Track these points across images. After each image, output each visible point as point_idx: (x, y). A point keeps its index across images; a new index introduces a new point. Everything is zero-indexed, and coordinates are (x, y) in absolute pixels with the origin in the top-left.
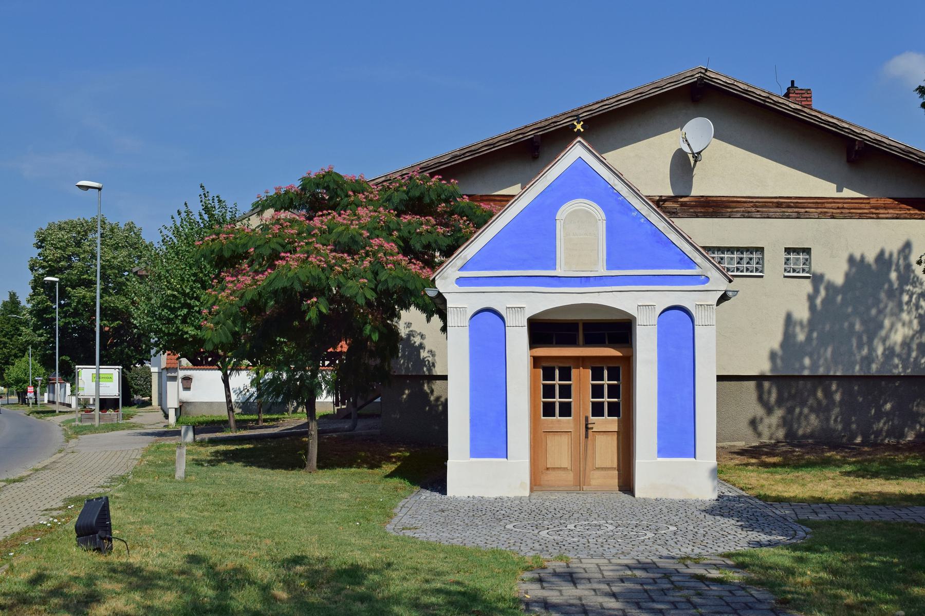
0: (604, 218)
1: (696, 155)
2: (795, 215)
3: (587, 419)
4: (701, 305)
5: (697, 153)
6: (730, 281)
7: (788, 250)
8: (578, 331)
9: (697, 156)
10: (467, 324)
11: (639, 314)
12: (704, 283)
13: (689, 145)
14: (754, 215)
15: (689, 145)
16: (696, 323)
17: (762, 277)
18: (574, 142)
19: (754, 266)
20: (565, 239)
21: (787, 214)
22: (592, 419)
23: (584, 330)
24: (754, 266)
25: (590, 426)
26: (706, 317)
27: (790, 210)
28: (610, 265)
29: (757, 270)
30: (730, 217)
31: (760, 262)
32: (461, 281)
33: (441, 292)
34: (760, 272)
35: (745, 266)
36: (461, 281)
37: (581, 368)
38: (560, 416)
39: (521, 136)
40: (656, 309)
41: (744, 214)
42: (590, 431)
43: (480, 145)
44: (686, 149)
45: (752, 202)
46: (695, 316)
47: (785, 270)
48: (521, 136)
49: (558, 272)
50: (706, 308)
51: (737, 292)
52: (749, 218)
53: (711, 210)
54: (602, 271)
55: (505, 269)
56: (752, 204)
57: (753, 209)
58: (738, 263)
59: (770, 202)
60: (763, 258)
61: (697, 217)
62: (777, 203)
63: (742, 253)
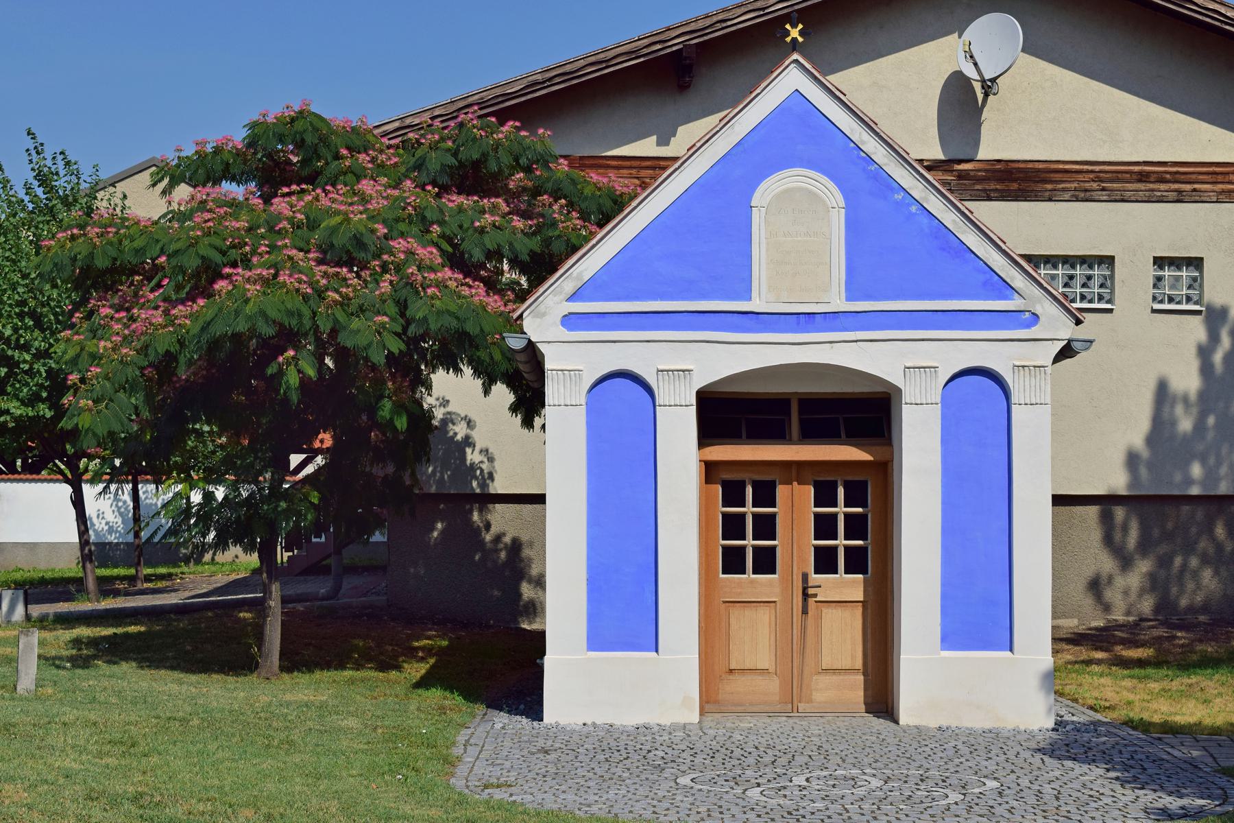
0: (842, 204)
1: (989, 83)
2: (1172, 195)
3: (805, 577)
4: (1023, 367)
5: (990, 80)
6: (1078, 322)
7: (1159, 262)
8: (789, 414)
9: (989, 87)
10: (583, 401)
11: (908, 383)
12: (1029, 325)
13: (976, 64)
14: (1096, 195)
15: (976, 64)
16: (1014, 399)
17: (1110, 311)
18: (787, 63)
19: (1096, 291)
20: (768, 244)
21: (1159, 194)
22: (815, 578)
23: (800, 413)
24: (1096, 291)
25: (811, 591)
26: (1033, 388)
27: (1163, 187)
28: (853, 290)
29: (1101, 298)
30: (1050, 200)
31: (1108, 282)
32: (570, 320)
33: (533, 339)
34: (1108, 302)
35: (1078, 291)
36: (570, 320)
37: (795, 483)
38: (754, 573)
39: (658, 47)
40: (940, 374)
41: (1077, 193)
42: (811, 601)
43: (582, 63)
44: (970, 72)
45: (1092, 172)
46: (1012, 388)
47: (1154, 298)
48: (658, 47)
49: (755, 305)
50: (1033, 373)
51: (1091, 342)
52: (1087, 200)
53: (1015, 186)
54: (838, 302)
56: (1092, 176)
57: (1095, 185)
58: (1066, 285)
59: (1126, 172)
60: (1112, 277)
61: (989, 199)
62: (1140, 173)
63: (1073, 267)
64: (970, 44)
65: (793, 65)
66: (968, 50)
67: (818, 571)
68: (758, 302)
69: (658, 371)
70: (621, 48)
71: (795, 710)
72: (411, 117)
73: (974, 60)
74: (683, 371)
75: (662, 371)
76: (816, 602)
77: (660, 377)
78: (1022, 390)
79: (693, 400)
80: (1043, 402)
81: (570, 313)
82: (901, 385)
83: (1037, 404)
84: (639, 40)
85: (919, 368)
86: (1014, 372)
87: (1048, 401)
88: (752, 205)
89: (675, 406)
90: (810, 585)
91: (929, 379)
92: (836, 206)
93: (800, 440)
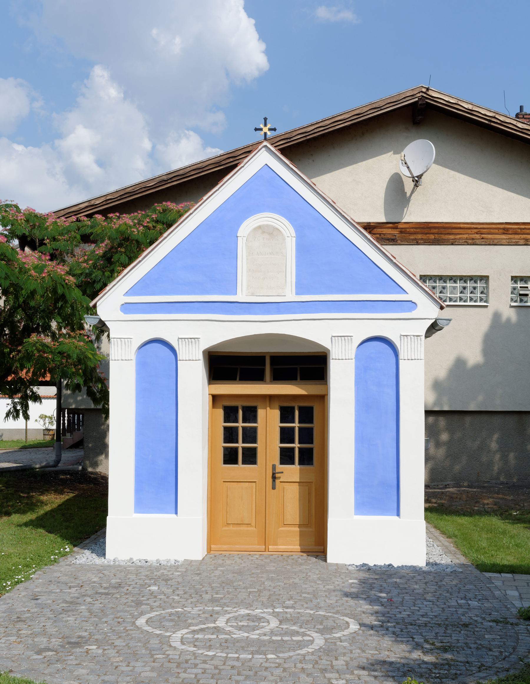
0: (294, 234)
1: (416, 179)
2: (522, 242)
3: (274, 467)
4: (407, 336)
5: (417, 177)
6: (442, 308)
7: (514, 279)
8: (264, 365)
9: (417, 181)
10: (133, 356)
11: (334, 346)
12: (410, 310)
13: (408, 168)
14: (478, 242)
15: (408, 168)
16: (401, 356)
17: (486, 306)
18: (260, 147)
19: (479, 295)
20: (247, 259)
21: (514, 241)
22: (280, 468)
23: (272, 364)
24: (479, 295)
25: (277, 475)
26: (413, 349)
27: (517, 236)
28: (300, 289)
29: (481, 300)
30: (452, 244)
31: (485, 292)
32: (127, 308)
33: (103, 319)
34: (485, 302)
35: (468, 295)
36: (127, 308)
37: (268, 408)
38: (243, 464)
39: (231, 160)
40: (353, 340)
41: (467, 240)
42: (277, 481)
43: (189, 169)
44: (404, 171)
45: (476, 228)
46: (399, 349)
47: (512, 300)
48: (231, 160)
49: (240, 297)
50: (413, 340)
51: (450, 320)
52: (473, 245)
53: (432, 237)
54: (290, 295)
55: (178, 294)
56: (476, 231)
57: (478, 236)
58: (461, 293)
59: (496, 229)
60: (487, 287)
61: (418, 244)
62: (504, 229)
63: (465, 282)
64: (404, 156)
65: (264, 149)
66: (403, 159)
67: (282, 463)
68: (241, 296)
69: (179, 338)
70: (211, 161)
71: (267, 550)
72: (94, 200)
73: (407, 165)
74: (194, 339)
75: (181, 339)
76: (281, 482)
77: (180, 343)
78: (406, 351)
79: (201, 357)
80: (419, 358)
81: (126, 303)
82: (329, 347)
83: (415, 359)
84: (220, 156)
85: (341, 337)
86: (401, 340)
87: (423, 357)
88: (238, 235)
89: (190, 360)
90: (277, 471)
91: (347, 343)
92: (290, 236)
93: (271, 382)
